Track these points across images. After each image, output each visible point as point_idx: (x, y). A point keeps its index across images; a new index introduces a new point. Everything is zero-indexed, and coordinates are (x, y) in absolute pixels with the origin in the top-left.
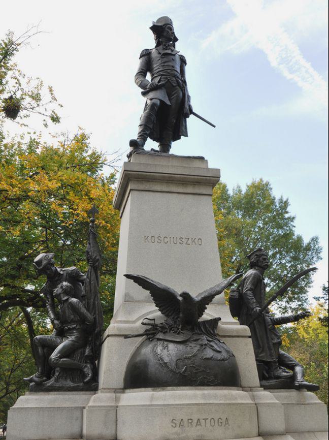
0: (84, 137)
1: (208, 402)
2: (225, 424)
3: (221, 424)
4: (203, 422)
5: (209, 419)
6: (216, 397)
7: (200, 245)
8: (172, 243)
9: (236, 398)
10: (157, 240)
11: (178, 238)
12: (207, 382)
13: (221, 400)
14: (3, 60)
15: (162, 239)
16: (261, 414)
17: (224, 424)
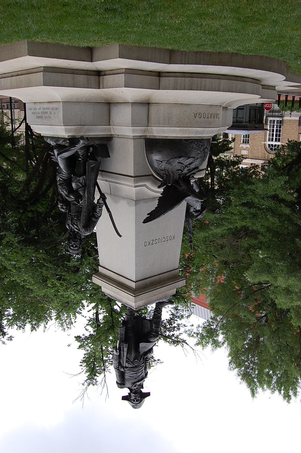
0: (36, 331)
1: (188, 128)
2: (196, 114)
3: (200, 114)
4: (209, 117)
5: (206, 118)
6: (197, 132)
7: (146, 242)
8: (161, 239)
9: (181, 130)
10: (168, 238)
11: (157, 243)
12: (195, 142)
13: (194, 130)
14: (171, 340)
15: (166, 241)
16: (145, 118)
17: (198, 113)
